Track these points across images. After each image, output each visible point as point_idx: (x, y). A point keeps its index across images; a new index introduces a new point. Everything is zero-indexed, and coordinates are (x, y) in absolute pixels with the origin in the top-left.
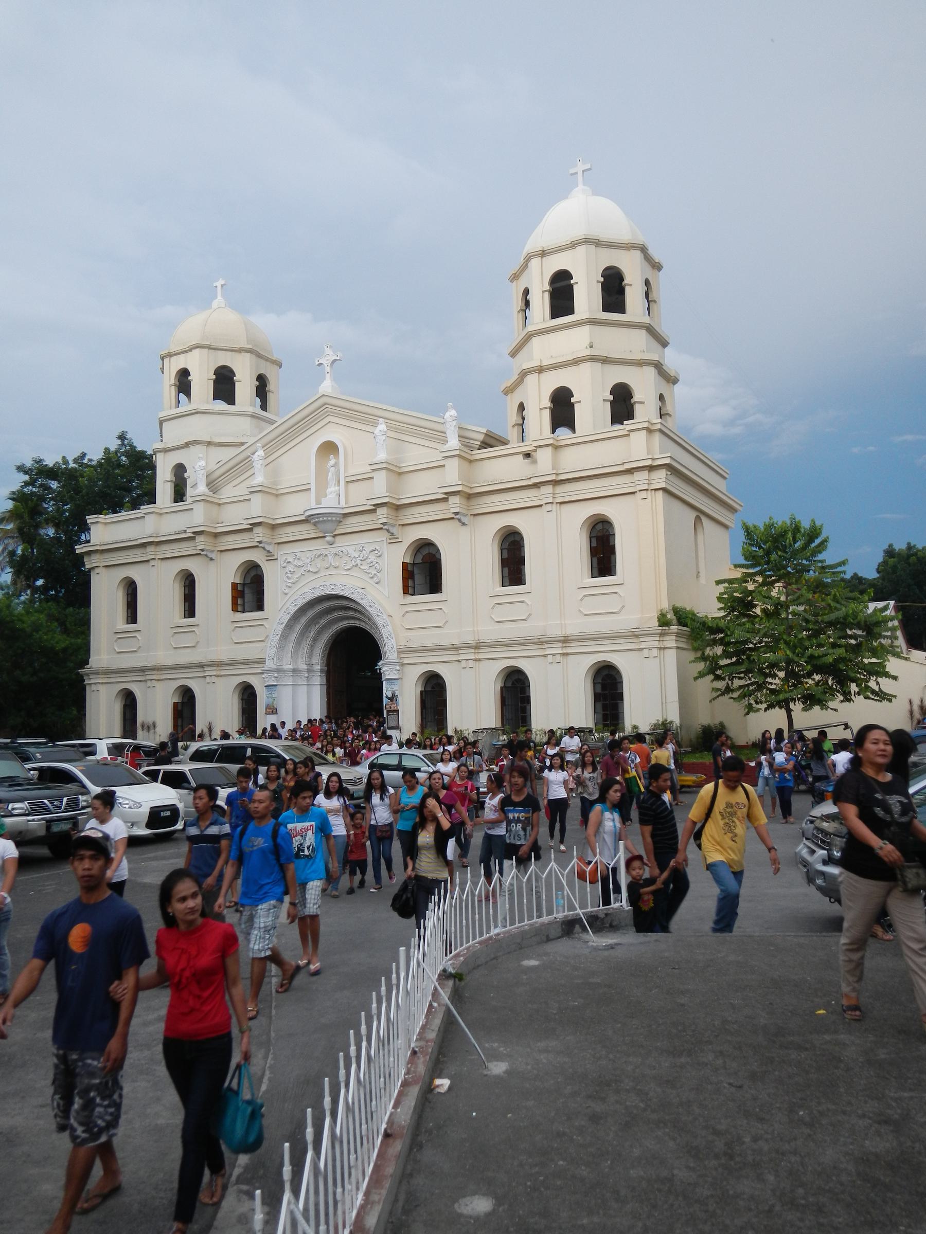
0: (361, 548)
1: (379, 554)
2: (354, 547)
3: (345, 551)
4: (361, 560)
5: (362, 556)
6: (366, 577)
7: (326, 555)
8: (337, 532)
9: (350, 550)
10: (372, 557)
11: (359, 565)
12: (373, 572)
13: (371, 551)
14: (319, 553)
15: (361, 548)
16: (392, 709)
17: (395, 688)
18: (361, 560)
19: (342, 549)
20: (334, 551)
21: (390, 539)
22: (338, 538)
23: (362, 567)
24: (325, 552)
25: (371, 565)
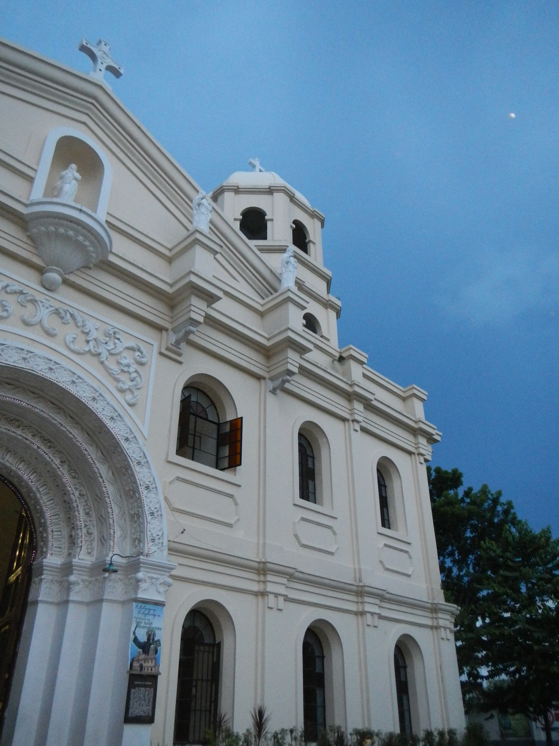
0: (111, 332)
1: (144, 360)
2: (98, 324)
3: (79, 319)
4: (108, 351)
5: (111, 346)
6: (111, 385)
7: (34, 301)
8: (72, 278)
9: (91, 325)
10: (128, 359)
11: (103, 357)
12: (128, 384)
13: (128, 348)
14: (17, 287)
15: (111, 332)
16: (145, 672)
17: (156, 623)
18: (108, 351)
19: (76, 313)
20: (57, 305)
21: (168, 349)
22: (65, 290)
23: (106, 363)
24: (38, 297)
25: (126, 369)
